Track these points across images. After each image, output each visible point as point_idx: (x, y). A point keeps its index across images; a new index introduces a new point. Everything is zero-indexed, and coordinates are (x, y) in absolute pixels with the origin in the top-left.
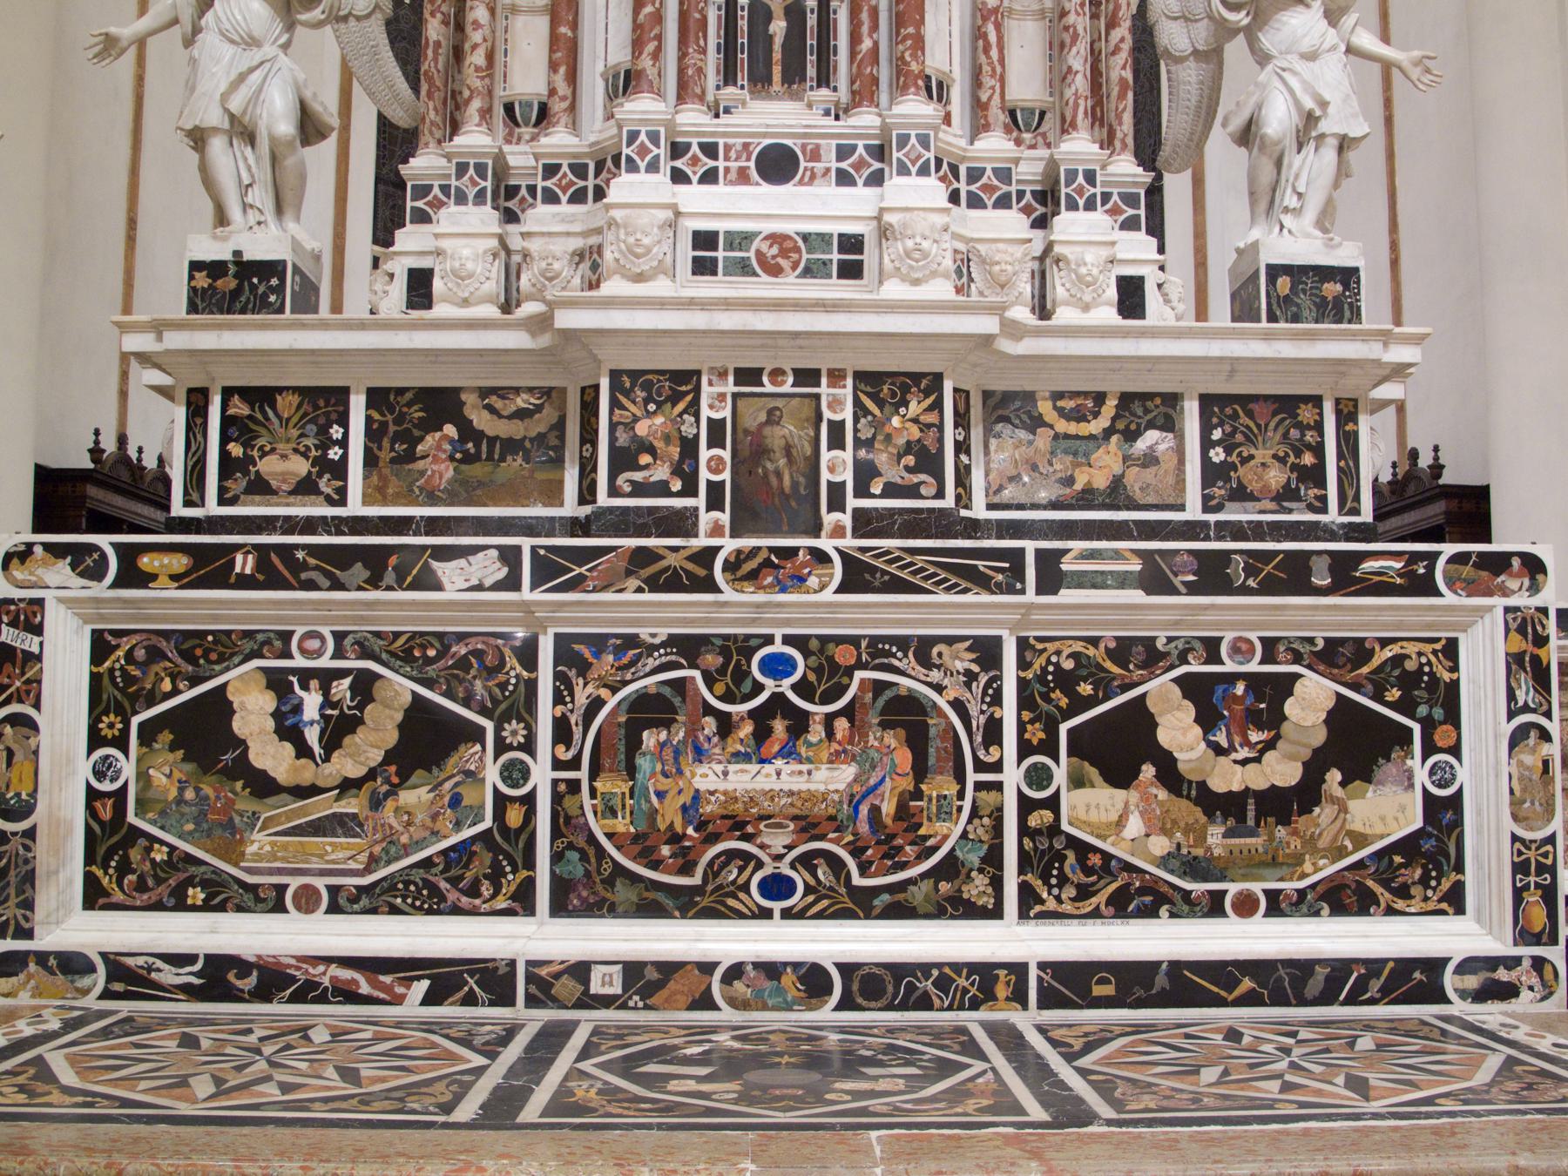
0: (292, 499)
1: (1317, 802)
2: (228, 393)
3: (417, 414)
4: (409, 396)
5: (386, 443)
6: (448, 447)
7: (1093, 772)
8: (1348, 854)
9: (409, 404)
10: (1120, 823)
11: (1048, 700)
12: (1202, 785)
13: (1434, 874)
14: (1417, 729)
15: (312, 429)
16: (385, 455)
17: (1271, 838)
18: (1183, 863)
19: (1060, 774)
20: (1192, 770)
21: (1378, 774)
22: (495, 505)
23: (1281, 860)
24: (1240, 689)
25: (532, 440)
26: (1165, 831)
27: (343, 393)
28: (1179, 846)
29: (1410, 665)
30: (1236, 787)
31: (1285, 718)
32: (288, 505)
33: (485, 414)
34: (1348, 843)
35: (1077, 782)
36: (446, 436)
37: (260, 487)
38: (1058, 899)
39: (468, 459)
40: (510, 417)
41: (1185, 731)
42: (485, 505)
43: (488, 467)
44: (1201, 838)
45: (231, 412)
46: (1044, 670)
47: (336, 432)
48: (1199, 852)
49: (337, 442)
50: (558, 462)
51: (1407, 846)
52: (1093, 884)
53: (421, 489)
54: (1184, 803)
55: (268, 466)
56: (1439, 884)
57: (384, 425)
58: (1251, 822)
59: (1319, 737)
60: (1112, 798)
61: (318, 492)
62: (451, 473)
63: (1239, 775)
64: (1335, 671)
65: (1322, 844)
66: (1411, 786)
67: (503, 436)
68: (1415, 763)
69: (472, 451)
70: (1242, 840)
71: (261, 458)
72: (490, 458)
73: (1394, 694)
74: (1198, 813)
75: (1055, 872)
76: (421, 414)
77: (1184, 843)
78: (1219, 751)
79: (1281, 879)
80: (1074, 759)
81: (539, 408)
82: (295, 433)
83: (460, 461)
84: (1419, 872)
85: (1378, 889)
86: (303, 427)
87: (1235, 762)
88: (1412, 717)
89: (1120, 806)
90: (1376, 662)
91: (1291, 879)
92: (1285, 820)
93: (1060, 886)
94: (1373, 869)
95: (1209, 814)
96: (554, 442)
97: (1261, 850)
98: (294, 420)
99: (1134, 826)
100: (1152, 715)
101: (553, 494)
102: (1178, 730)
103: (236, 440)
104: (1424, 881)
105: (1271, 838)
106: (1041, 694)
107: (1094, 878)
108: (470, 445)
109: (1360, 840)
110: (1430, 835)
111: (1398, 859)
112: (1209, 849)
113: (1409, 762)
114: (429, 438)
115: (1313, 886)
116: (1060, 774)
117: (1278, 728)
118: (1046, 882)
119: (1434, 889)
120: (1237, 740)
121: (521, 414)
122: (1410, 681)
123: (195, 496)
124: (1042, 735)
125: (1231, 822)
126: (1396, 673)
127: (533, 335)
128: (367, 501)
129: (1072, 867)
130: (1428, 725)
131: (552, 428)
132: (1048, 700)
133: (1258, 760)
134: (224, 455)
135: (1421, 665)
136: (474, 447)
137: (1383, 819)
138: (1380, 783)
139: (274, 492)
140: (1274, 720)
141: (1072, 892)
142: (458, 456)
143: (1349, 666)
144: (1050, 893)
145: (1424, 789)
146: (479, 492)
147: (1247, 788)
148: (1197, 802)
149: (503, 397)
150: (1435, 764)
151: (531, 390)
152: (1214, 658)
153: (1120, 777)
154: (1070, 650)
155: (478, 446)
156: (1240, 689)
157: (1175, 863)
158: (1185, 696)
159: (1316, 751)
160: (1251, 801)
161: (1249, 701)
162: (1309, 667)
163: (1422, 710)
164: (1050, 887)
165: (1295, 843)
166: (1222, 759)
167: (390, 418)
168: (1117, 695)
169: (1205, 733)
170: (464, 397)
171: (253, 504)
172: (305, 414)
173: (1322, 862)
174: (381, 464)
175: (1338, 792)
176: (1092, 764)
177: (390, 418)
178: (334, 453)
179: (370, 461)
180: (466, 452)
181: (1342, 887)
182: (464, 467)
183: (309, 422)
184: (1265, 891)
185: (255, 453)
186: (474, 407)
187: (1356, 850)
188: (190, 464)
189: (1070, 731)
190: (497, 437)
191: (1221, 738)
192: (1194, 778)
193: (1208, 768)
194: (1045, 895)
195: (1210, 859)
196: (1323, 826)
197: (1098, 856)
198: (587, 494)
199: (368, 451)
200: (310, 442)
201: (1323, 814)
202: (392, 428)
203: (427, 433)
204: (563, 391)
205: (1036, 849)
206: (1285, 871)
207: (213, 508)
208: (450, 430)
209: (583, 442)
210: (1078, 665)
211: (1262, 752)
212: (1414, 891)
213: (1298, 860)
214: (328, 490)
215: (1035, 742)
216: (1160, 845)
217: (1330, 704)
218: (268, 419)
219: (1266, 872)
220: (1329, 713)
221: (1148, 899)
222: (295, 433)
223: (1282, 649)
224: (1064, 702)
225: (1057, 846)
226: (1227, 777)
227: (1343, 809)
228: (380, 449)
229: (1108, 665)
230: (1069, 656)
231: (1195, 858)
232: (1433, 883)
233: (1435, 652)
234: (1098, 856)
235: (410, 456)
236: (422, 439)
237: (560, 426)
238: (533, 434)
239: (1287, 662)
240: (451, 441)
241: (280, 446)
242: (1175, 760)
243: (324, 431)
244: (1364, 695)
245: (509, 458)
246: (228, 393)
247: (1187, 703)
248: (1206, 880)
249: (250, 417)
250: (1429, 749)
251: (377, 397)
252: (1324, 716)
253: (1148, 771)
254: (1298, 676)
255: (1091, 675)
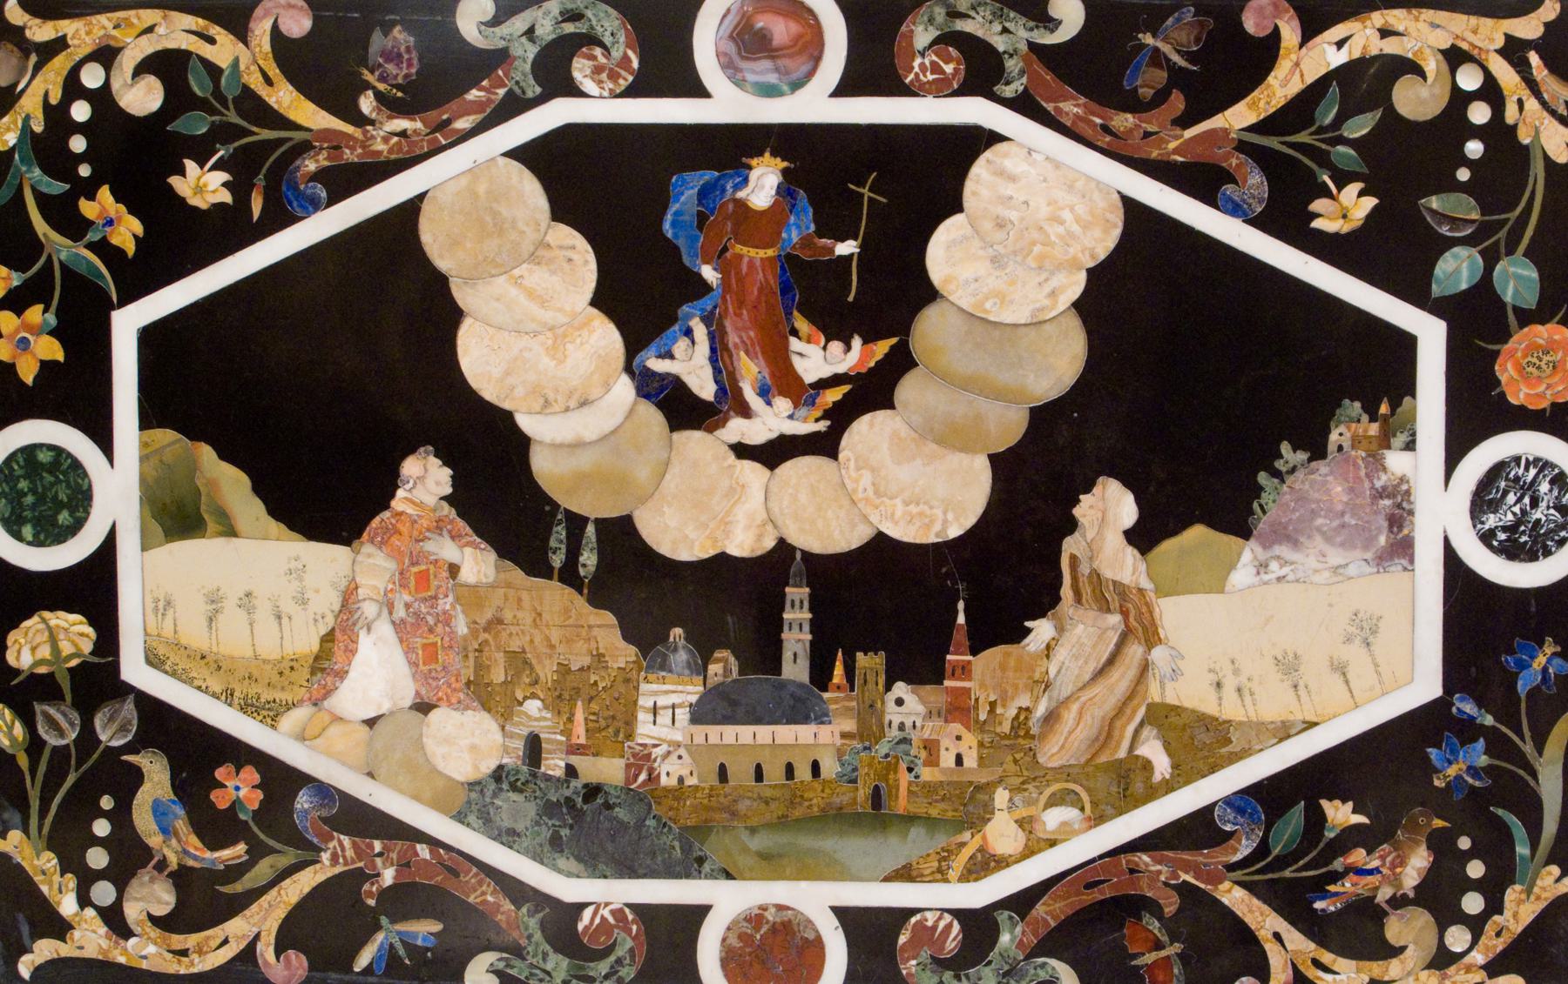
1: (1044, 600)
7: (230, 483)
8: (1153, 792)
10: (327, 661)
11: (74, 226)
12: (620, 535)
13: (1476, 870)
14: (1431, 337)
17: (870, 729)
18: (550, 809)
19: (117, 486)
20: (582, 480)
21: (1277, 501)
23: (902, 804)
24: (762, 184)
26: (484, 695)
28: (534, 748)
29: (1416, 100)
30: (744, 543)
31: (928, 294)
34: (1154, 752)
35: (177, 514)
38: (114, 920)
41: (558, 337)
44: (616, 724)
46: (57, 115)
48: (608, 770)
51: (1379, 766)
52: (235, 872)
54: (555, 594)
56: (1495, 905)
58: (796, 668)
59: (1058, 363)
60: (297, 572)
63: (753, 501)
64: (1124, 121)
65: (1055, 752)
66: (1403, 548)
68: (1419, 463)
70: (764, 733)
73: (1347, 208)
74: (604, 629)
75: (101, 828)
77: (552, 738)
78: (682, 409)
79: (905, 874)
80: (165, 436)
84: (1418, 862)
85: (1264, 920)
87: (742, 451)
88: (1417, 294)
89: (327, 601)
90: (1281, 86)
91: (941, 875)
92: (920, 662)
93: (121, 875)
94: (1245, 848)
95: (647, 639)
97: (830, 768)
99: (378, 674)
100: (440, 282)
102: (533, 330)
104: (1438, 897)
105: (870, 729)
106: (43, 201)
107: (236, 852)
109: (1200, 741)
110: (1467, 731)
111: (1340, 814)
112: (642, 760)
113: (1396, 461)
115: (1022, 902)
116: (117, 486)
117: (902, 327)
118: (71, 862)
119: (1476, 925)
120: (750, 371)
122: (1410, 159)
124: (51, 349)
125: (723, 666)
126: (1360, 127)
129: (158, 810)
130: (1477, 323)
132: (74, 226)
133: (825, 445)
135: (1460, 99)
137: (1288, 666)
138: (1286, 535)
140: (885, 298)
141: (163, 898)
143: (1178, 102)
144: (84, 901)
145: (1453, 563)
147: (783, 546)
148: (600, 593)
150: (1497, 470)
152: (668, 70)
153: (328, 497)
154: (148, 46)
156: (762, 184)
157: (516, 808)
158: (561, 212)
159: (1043, 417)
160: (797, 593)
161: (798, 229)
162: (1025, 105)
163: (1456, 269)
164: (86, 879)
165: (959, 747)
166: (693, 440)
168: (315, 205)
169: (634, 344)
173: (1054, 818)
175: (1124, 565)
176: (225, 455)
181: (1131, 906)
184: (841, 913)
187: (1183, 775)
189: (150, 337)
191: (690, 364)
192: (594, 505)
193: (643, 473)
194: (68, 906)
195: (646, 794)
196: (1064, 688)
197: (251, 775)
201: (1065, 643)
205: (35, 745)
206: (914, 845)
210: (178, 99)
211: (841, 417)
212: (1395, 930)
213: (969, 807)
215: (28, 373)
216: (468, 743)
217: (1103, 241)
219: (851, 847)
220: (1095, 275)
221: (424, 930)
223: (922, 36)
224: (127, 232)
225: (109, 734)
226: (709, 506)
227: (1141, 628)
229: (285, 98)
230: (142, 68)
231: (593, 791)
232: (1473, 903)
233: (1514, 50)
234: (251, 775)
239: (942, 89)
242: (522, 443)
244: (1234, 209)
247: (569, 239)
248: (628, 870)
250: (1477, 411)
252: (1076, 285)
253: (425, 480)
254: (978, 140)
255: (223, 133)
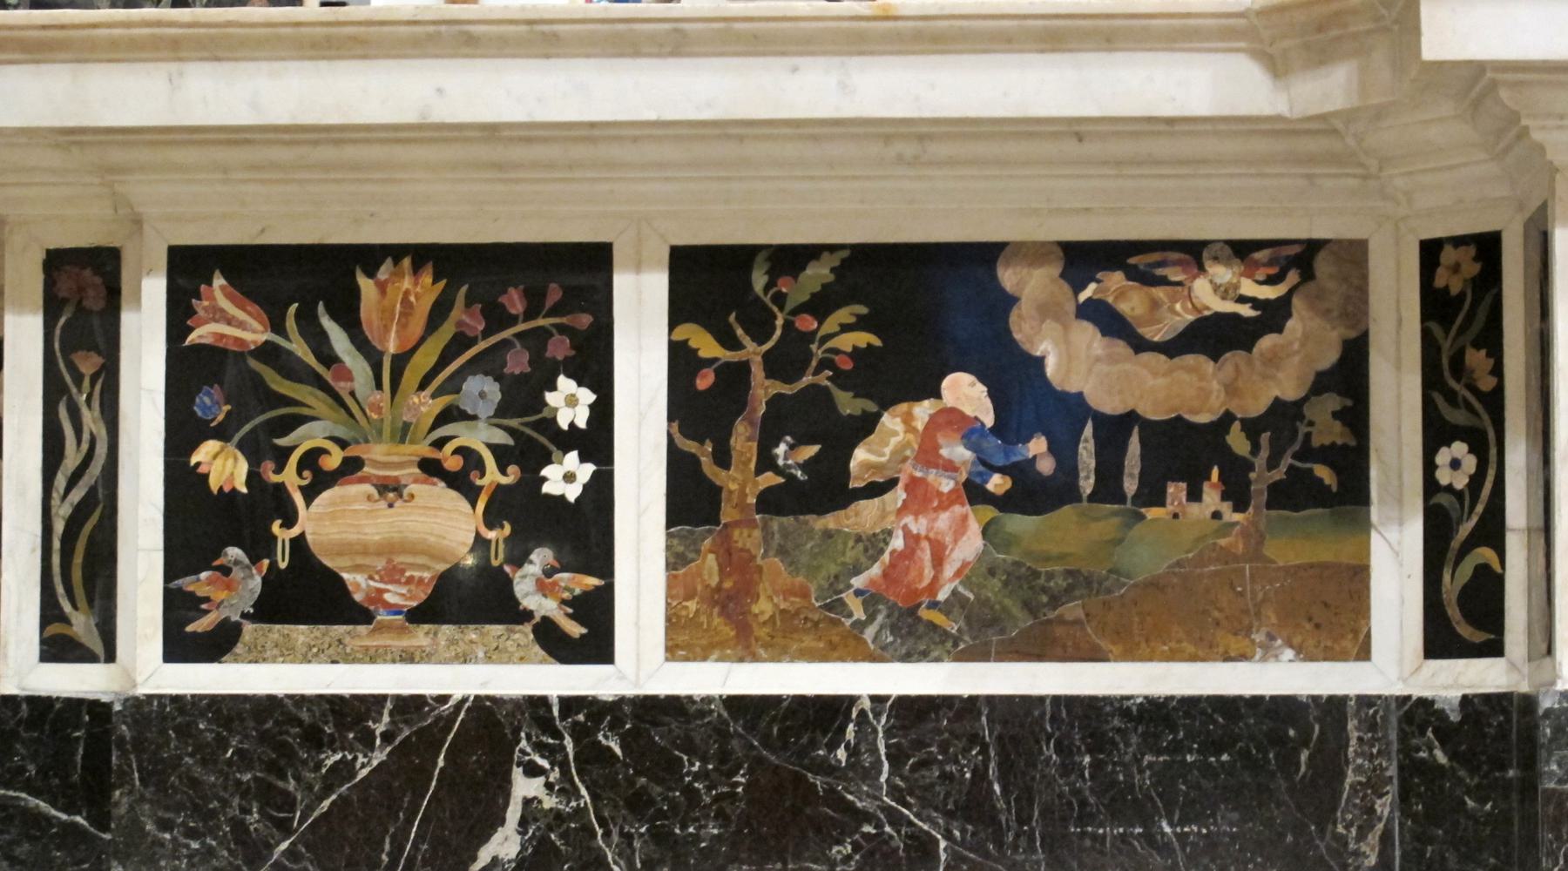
0: (421, 636)
2: (189, 268)
3: (846, 336)
4: (818, 274)
5: (743, 440)
6: (960, 453)
9: (820, 305)
15: (482, 392)
16: (741, 482)
22: (1130, 655)
25: (1252, 428)
27: (588, 267)
32: (408, 657)
33: (1087, 336)
36: (952, 419)
37: (310, 596)
39: (1032, 494)
40: (1172, 348)
42: (1095, 655)
43: (1105, 522)
45: (201, 334)
47: (569, 403)
49: (570, 439)
50: (1350, 496)
53: (871, 600)
55: (333, 523)
57: (734, 378)
61: (512, 613)
62: (970, 546)
67: (1153, 412)
69: (1046, 466)
71: (310, 494)
72: (1108, 488)
76: (863, 339)
81: (1273, 316)
82: (426, 406)
83: (1005, 503)
86: (453, 385)
96: (1326, 428)
98: (425, 359)
101: (1338, 621)
103: (222, 433)
108: (1037, 446)
114: (890, 421)
121: (1214, 337)
123: (81, 624)
127: (1277, 67)
128: (683, 640)
131: (1322, 384)
134: (182, 483)
136: (1049, 457)
139: (360, 615)
142: (997, 483)
146: (1072, 610)
149: (1147, 279)
151: (1241, 250)
155: (1064, 451)
167: (753, 352)
170: (1008, 277)
171: (287, 653)
172: (460, 342)
174: (728, 514)
177: (753, 352)
178: (565, 477)
179: (690, 500)
180: (1021, 472)
182: (1019, 524)
183: (473, 367)
185: (290, 478)
186: (1046, 311)
188: (62, 512)
190: (1130, 419)
198: (1464, 614)
199: (681, 470)
200: (480, 437)
202: (763, 389)
203: (886, 405)
204: (1354, 254)
207: (142, 667)
208: (965, 392)
209: (1436, 434)
214: (544, 606)
218: (329, 359)
222: (426, 406)
228: (723, 458)
235: (828, 488)
236: (865, 426)
237: (1348, 377)
238: (1256, 407)
240: (970, 432)
241: (377, 453)
243: (524, 398)
245: (1176, 491)
246: (189, 268)
249: (268, 353)
251: (709, 282)
